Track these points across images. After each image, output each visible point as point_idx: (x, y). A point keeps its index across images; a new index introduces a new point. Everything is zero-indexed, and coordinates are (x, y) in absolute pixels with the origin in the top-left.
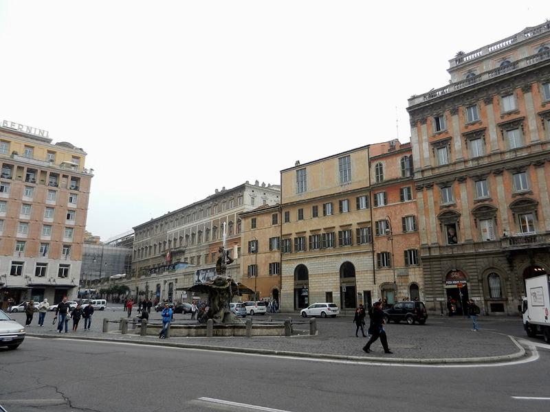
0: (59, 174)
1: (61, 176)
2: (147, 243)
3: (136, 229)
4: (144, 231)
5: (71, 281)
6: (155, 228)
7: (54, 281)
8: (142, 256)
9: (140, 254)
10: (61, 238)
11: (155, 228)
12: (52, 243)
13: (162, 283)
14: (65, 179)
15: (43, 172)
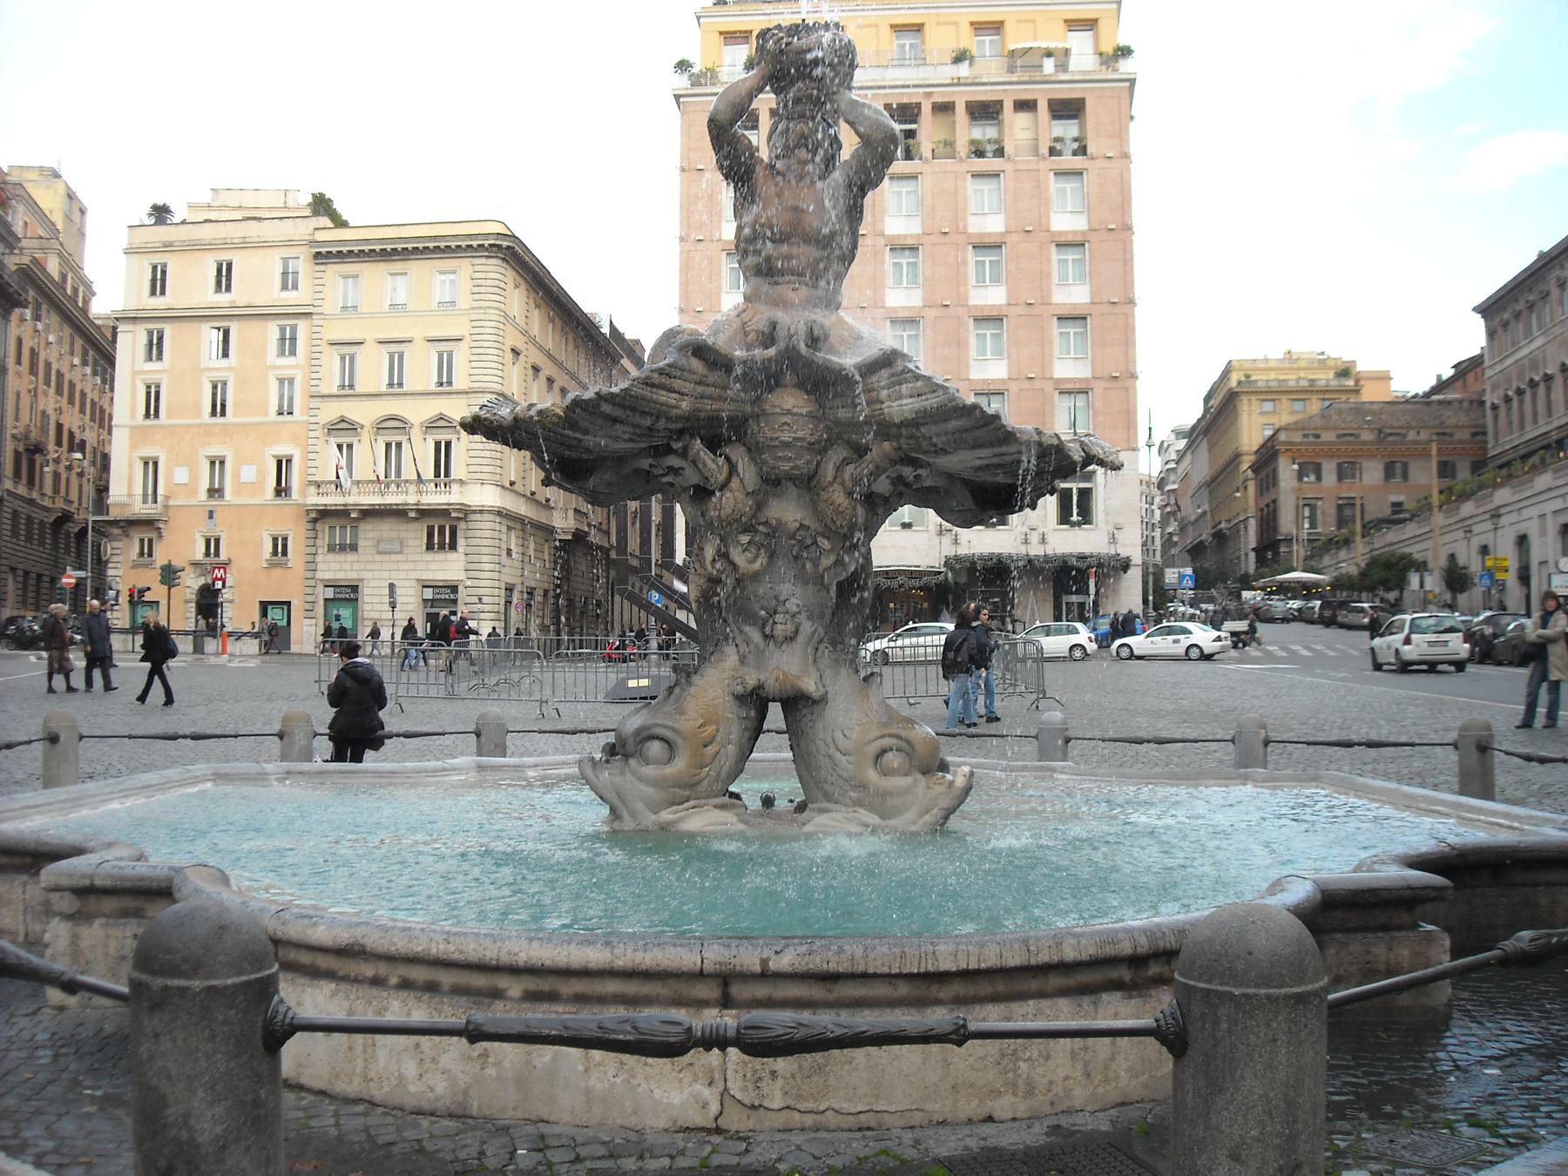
0: (1000, 103)
1: (1008, 107)
2: (1534, 365)
3: (1488, 310)
4: (1517, 315)
5: (1106, 538)
6: (1555, 291)
7: (1043, 541)
8: (1522, 427)
9: (1515, 417)
10: (1045, 363)
11: (1555, 291)
12: (1014, 388)
13: (1532, 529)
14: (1023, 119)
15: (944, 108)
